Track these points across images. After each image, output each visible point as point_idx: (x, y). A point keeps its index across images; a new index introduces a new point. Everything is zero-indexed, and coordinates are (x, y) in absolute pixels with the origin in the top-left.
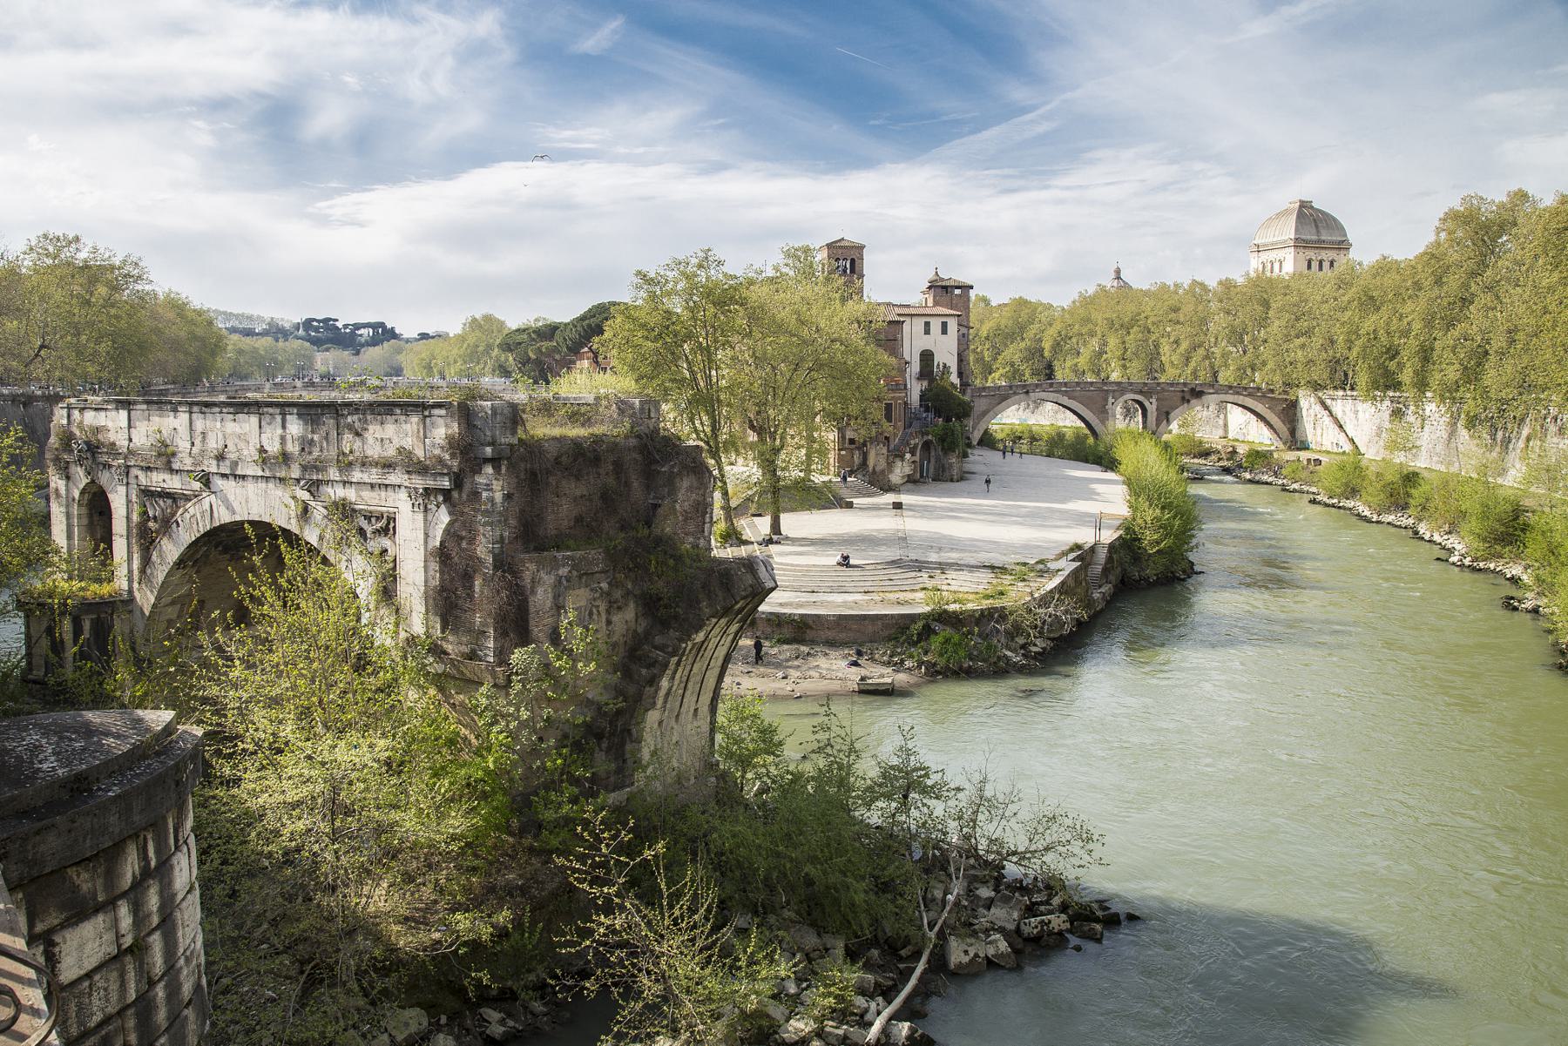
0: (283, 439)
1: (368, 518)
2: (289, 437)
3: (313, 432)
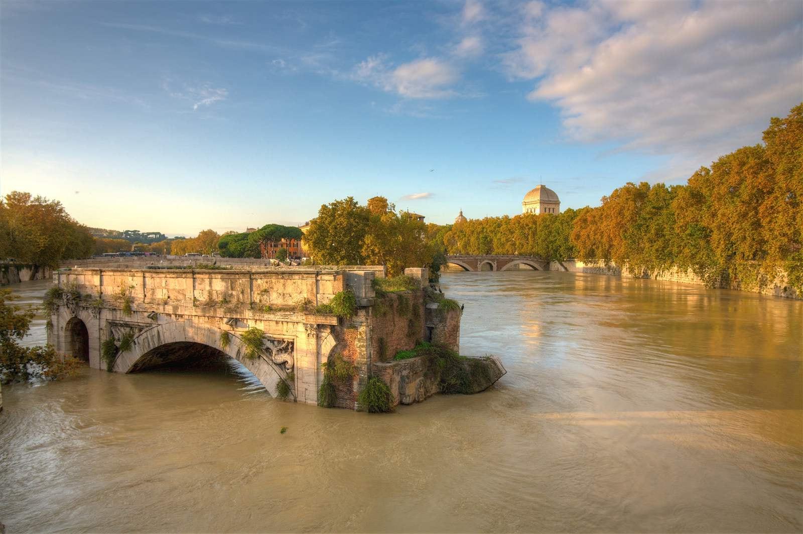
0: (210, 293)
1: (273, 342)
2: (214, 292)
3: (232, 289)
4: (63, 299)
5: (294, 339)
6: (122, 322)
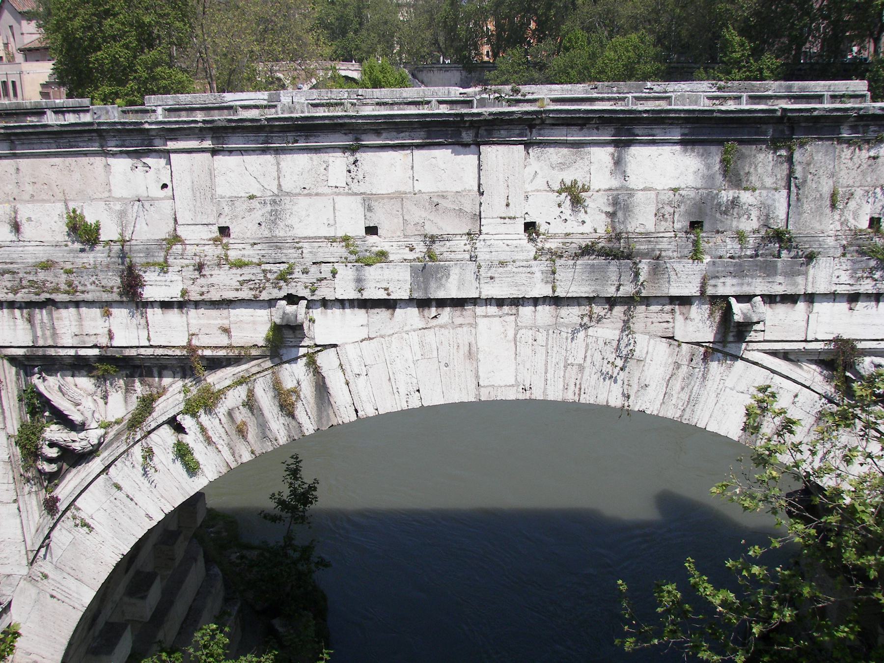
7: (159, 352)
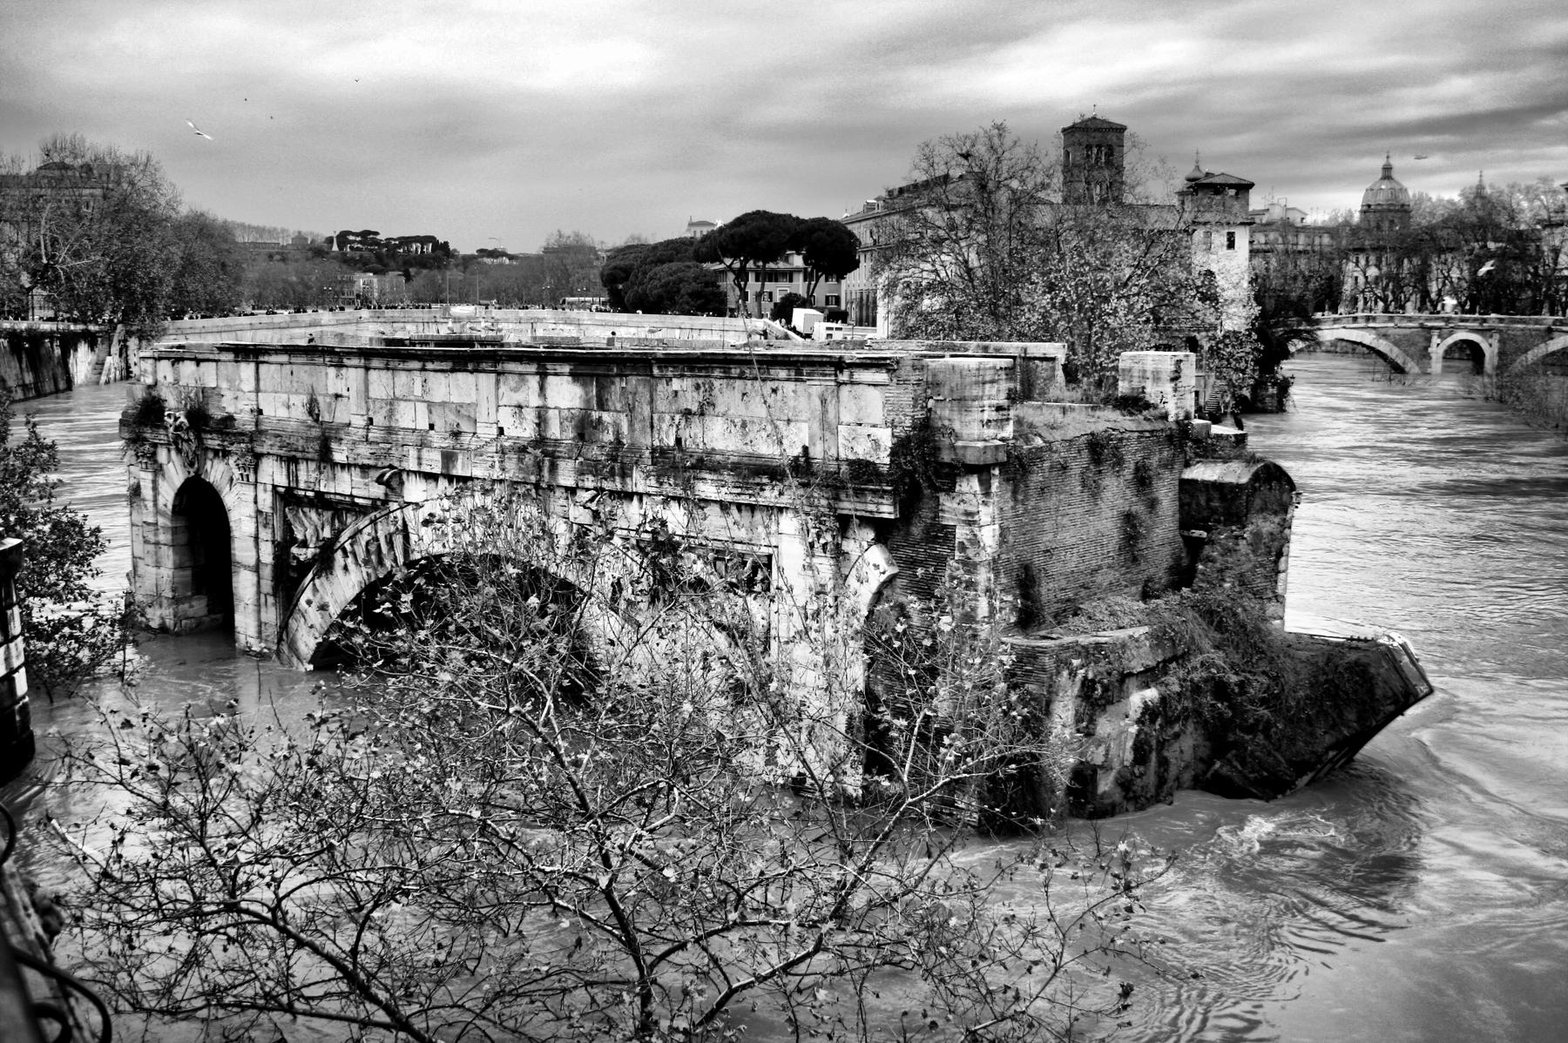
2: (553, 415)
3: (602, 406)
4: (166, 428)
5: (770, 557)
6: (311, 494)
7: (338, 497)
